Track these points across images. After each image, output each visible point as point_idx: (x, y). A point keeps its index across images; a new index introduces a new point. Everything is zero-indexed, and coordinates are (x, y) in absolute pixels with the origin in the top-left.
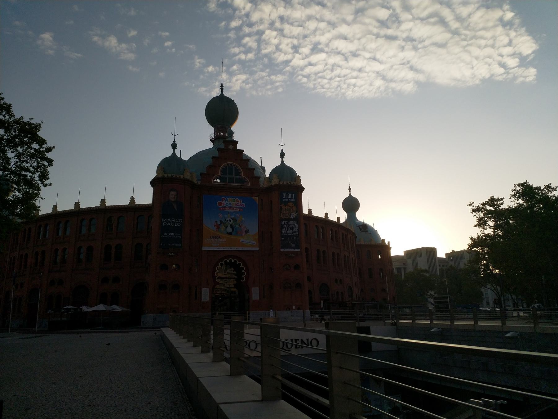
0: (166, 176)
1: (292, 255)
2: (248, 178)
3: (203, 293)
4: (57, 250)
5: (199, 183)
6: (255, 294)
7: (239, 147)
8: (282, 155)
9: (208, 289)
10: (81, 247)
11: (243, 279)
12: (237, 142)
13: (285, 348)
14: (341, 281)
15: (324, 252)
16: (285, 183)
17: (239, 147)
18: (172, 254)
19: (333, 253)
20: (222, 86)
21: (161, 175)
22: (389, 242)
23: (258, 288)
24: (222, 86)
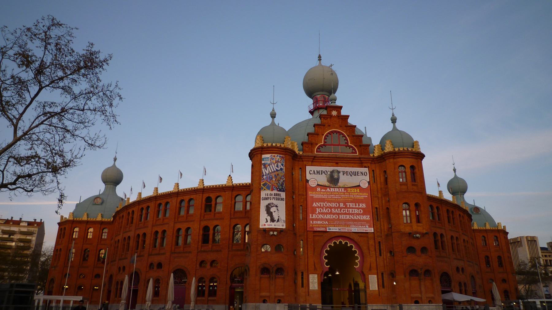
0: (265, 145)
1: (418, 235)
2: (355, 146)
3: (310, 280)
4: (157, 232)
5: (301, 153)
7: (343, 112)
8: (394, 120)
9: (316, 276)
10: (179, 229)
11: (357, 264)
12: (341, 108)
15: (442, 235)
16: (401, 149)
17: (343, 112)
19: (452, 237)
20: (320, 57)
21: (260, 145)
22: (504, 227)
23: (376, 276)
24: (320, 57)
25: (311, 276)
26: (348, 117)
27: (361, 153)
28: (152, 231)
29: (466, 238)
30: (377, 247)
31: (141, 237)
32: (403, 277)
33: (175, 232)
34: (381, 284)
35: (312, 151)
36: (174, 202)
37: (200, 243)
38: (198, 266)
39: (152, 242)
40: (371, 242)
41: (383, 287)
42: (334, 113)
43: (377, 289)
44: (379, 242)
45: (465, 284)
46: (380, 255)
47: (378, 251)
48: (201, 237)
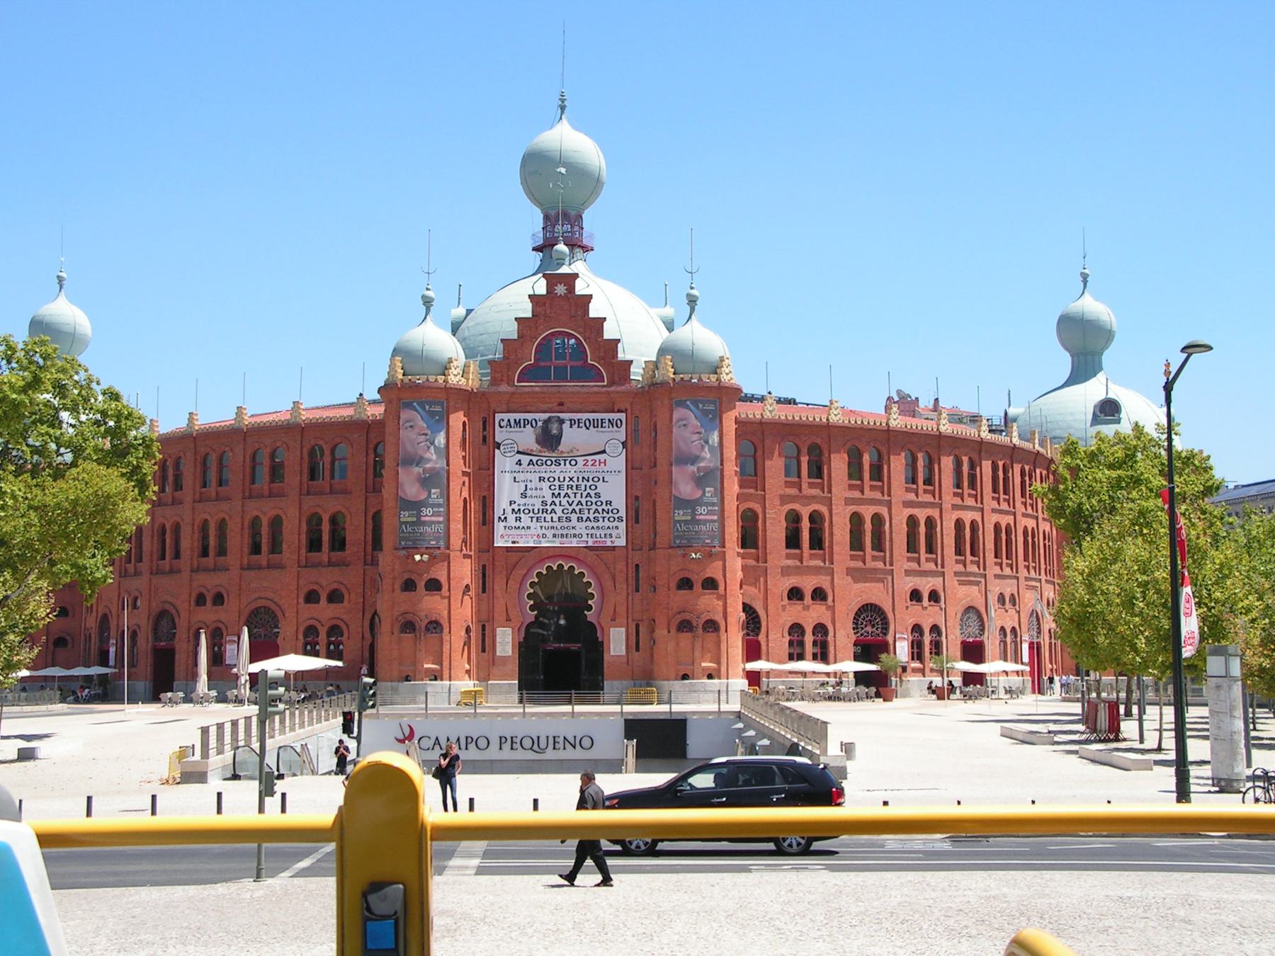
3: (498, 639)
6: (616, 642)
9: (509, 630)
11: (590, 608)
13: (536, 747)
14: (934, 596)
18: (426, 557)
25: (499, 630)
26: (588, 298)
27: (612, 383)
28: (193, 519)
29: (968, 517)
30: (632, 574)
31: (168, 531)
32: (665, 632)
33: (246, 524)
34: (635, 644)
35: (510, 382)
36: (237, 458)
37: (304, 551)
38: (301, 600)
39: (196, 544)
40: (621, 566)
41: (637, 649)
42: (561, 289)
43: (624, 653)
44: (637, 566)
45: (935, 629)
46: (637, 591)
47: (632, 582)
48: (304, 536)
